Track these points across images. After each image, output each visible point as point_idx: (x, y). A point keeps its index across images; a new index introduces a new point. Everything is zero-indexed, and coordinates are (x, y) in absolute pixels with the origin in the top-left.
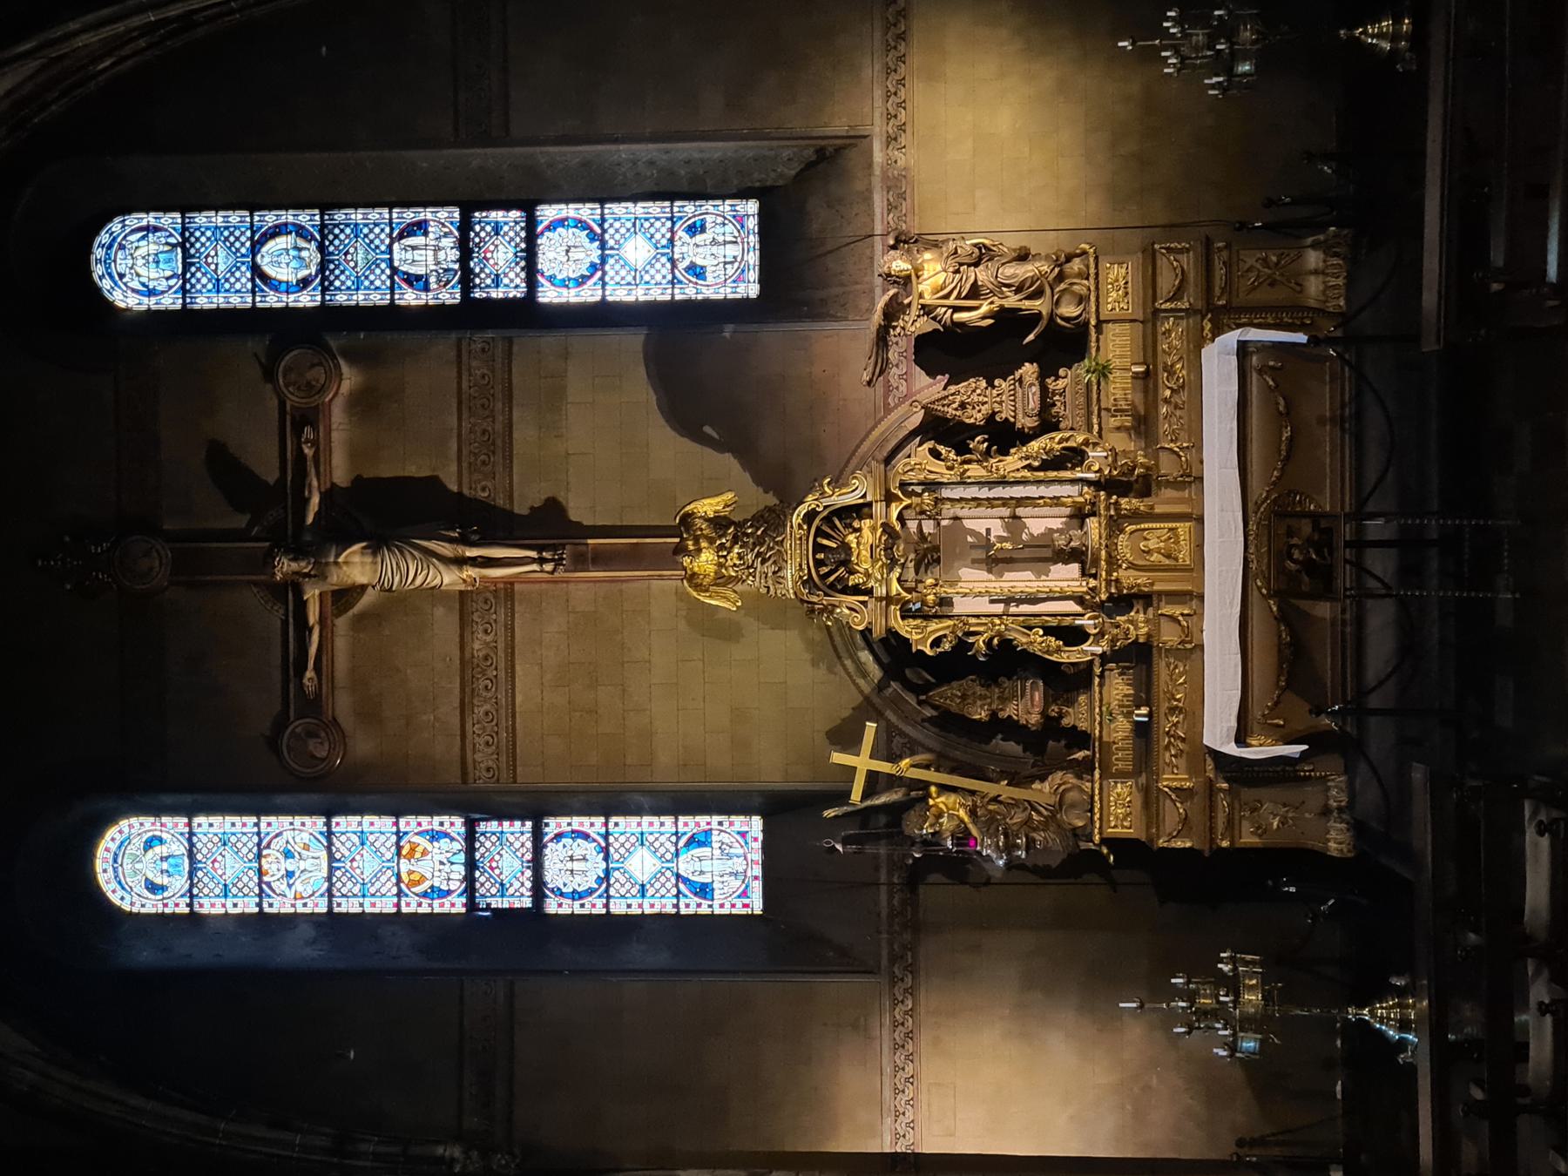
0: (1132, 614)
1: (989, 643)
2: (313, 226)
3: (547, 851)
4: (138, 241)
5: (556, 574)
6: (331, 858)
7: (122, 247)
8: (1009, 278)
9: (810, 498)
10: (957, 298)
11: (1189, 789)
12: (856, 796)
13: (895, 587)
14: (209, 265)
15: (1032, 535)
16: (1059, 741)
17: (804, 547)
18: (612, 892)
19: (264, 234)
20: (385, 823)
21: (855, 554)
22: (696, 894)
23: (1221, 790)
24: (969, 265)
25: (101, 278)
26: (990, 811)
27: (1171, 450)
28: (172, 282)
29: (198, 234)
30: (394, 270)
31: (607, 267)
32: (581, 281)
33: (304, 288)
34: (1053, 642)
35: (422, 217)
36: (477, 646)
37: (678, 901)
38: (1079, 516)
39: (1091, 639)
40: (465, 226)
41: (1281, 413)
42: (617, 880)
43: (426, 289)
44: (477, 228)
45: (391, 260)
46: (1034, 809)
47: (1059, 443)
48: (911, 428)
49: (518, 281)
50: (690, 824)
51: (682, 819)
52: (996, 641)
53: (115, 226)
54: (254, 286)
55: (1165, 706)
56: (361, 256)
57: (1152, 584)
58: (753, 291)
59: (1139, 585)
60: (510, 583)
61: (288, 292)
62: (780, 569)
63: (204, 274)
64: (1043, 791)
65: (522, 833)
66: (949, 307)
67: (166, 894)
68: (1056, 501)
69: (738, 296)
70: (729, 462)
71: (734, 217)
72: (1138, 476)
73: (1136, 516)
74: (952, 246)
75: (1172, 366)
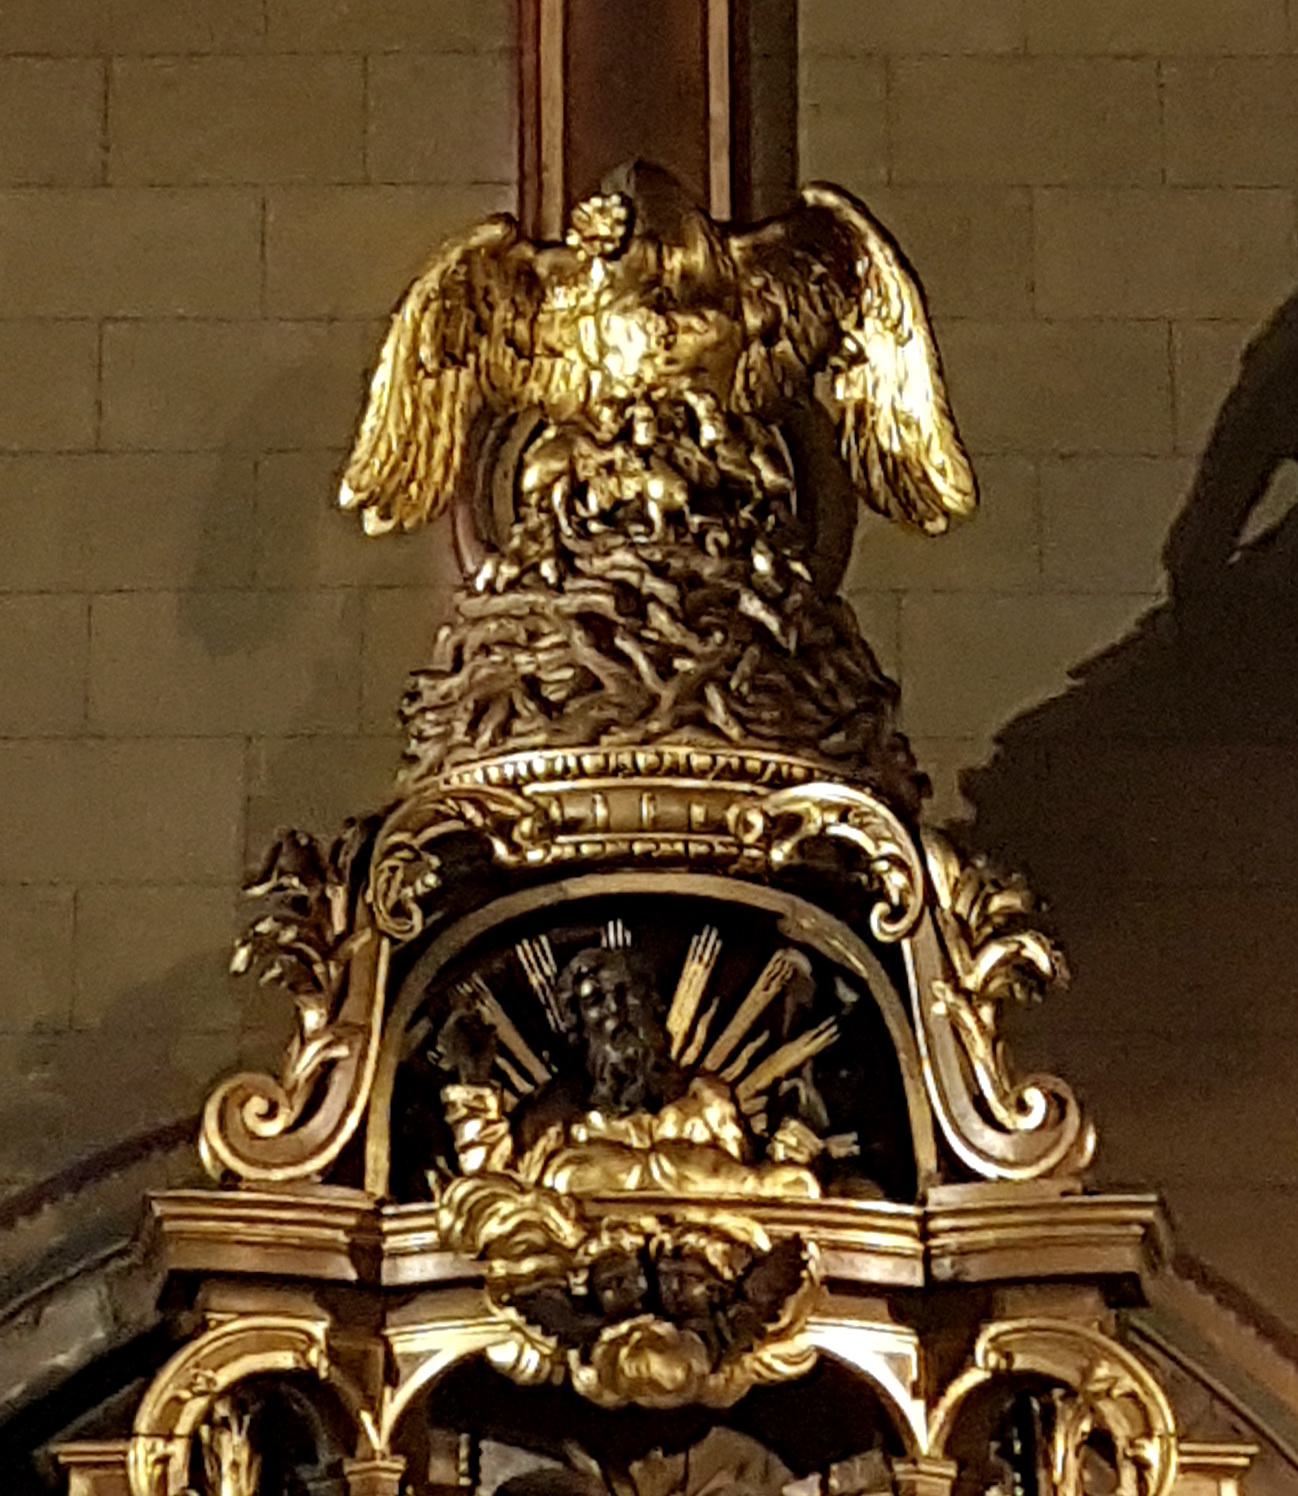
62: (550, 709)
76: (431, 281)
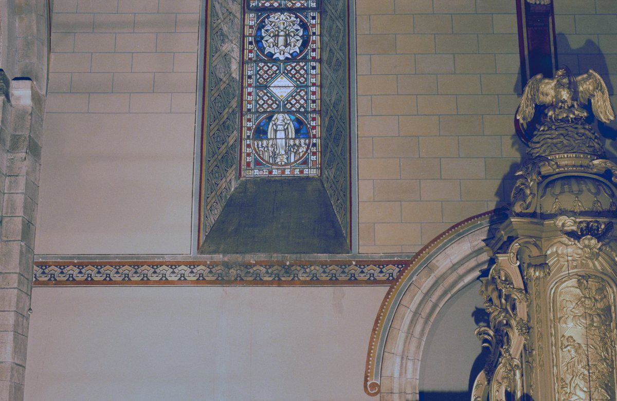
37: (253, 113)
42: (270, 68)
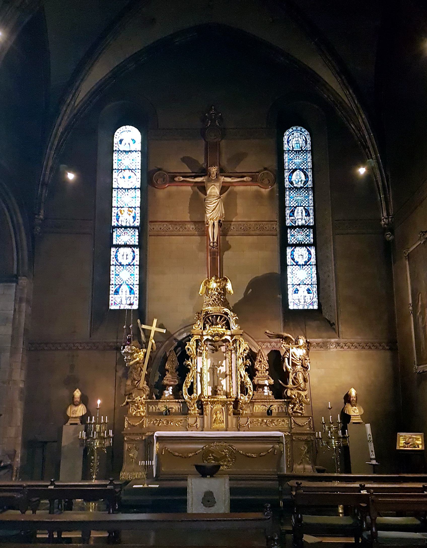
0: (197, 409)
1: (189, 365)
2: (308, 185)
3: (129, 248)
4: (303, 139)
5: (209, 246)
6: (128, 189)
7: (301, 134)
8: (298, 375)
9: (232, 313)
10: (292, 359)
11: (143, 427)
12: (144, 326)
13: (205, 338)
14: (297, 157)
15: (221, 381)
16: (159, 393)
17: (217, 312)
18: (117, 266)
19: (305, 172)
20: (138, 204)
21: (215, 327)
22: (116, 290)
23: (143, 437)
24: (302, 363)
25: (292, 129)
26: (138, 368)
27: (248, 421)
28: (291, 147)
29: (305, 154)
30: (295, 207)
31: (297, 266)
32: (293, 259)
33: (290, 183)
34: (189, 384)
35: (311, 215)
36: (189, 226)
38: (227, 394)
39: (190, 396)
40: (308, 227)
41: (260, 453)
43: (290, 216)
44: (308, 230)
45: (298, 206)
46: (138, 381)
47: (249, 387)
48: (252, 349)
49: (293, 241)
50: (136, 289)
51: (138, 286)
52: (189, 367)
53: (307, 133)
54: (291, 170)
55: (168, 419)
56: (299, 198)
57: (206, 415)
58: (291, 307)
59: (206, 411)
60: (208, 235)
61: (289, 178)
63: (293, 156)
64: (143, 384)
65: (135, 242)
66: (289, 357)
67: (119, 144)
68: (231, 387)
69: (289, 303)
70: (241, 296)
71: (313, 302)
72: (239, 411)
73: (228, 410)
74: (308, 359)
75: (274, 423)
76: (204, 281)
